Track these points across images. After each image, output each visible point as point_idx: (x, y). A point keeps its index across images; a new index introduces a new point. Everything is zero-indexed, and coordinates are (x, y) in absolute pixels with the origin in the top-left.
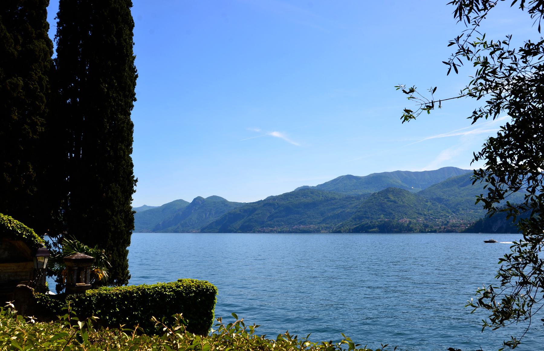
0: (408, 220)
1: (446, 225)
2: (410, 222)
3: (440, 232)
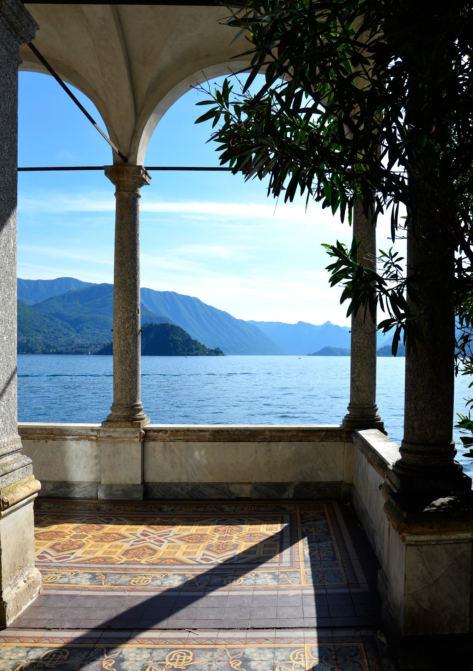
0: (25, 338)
1: (70, 345)
2: (28, 341)
3: (67, 353)
